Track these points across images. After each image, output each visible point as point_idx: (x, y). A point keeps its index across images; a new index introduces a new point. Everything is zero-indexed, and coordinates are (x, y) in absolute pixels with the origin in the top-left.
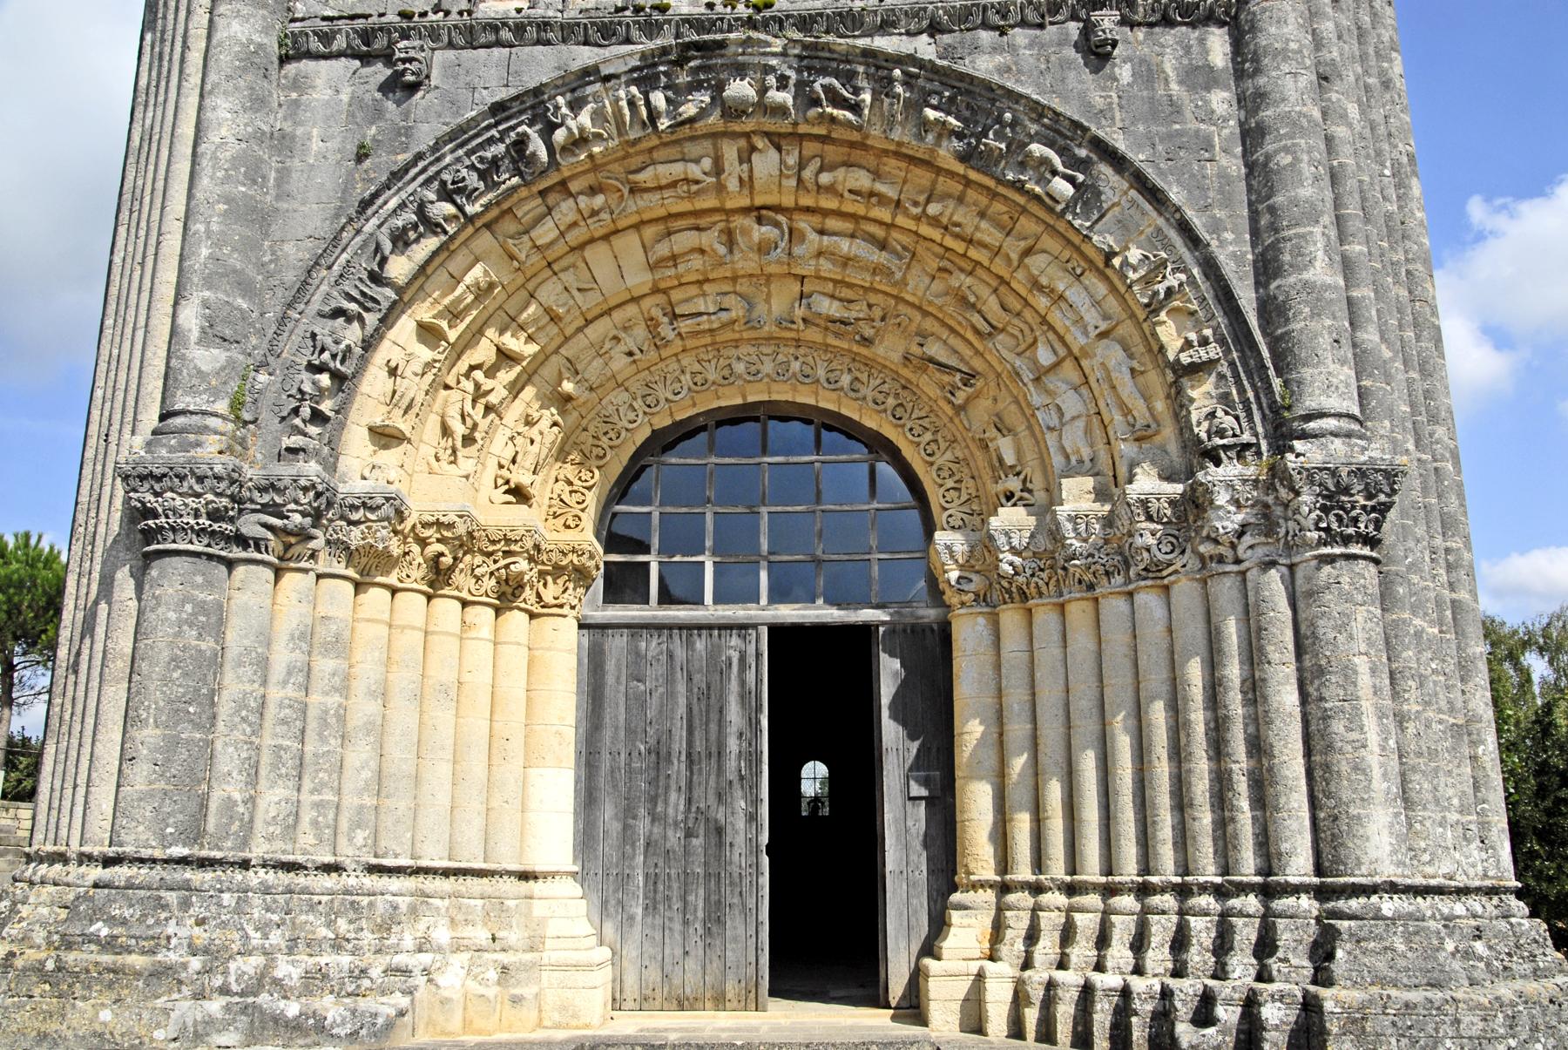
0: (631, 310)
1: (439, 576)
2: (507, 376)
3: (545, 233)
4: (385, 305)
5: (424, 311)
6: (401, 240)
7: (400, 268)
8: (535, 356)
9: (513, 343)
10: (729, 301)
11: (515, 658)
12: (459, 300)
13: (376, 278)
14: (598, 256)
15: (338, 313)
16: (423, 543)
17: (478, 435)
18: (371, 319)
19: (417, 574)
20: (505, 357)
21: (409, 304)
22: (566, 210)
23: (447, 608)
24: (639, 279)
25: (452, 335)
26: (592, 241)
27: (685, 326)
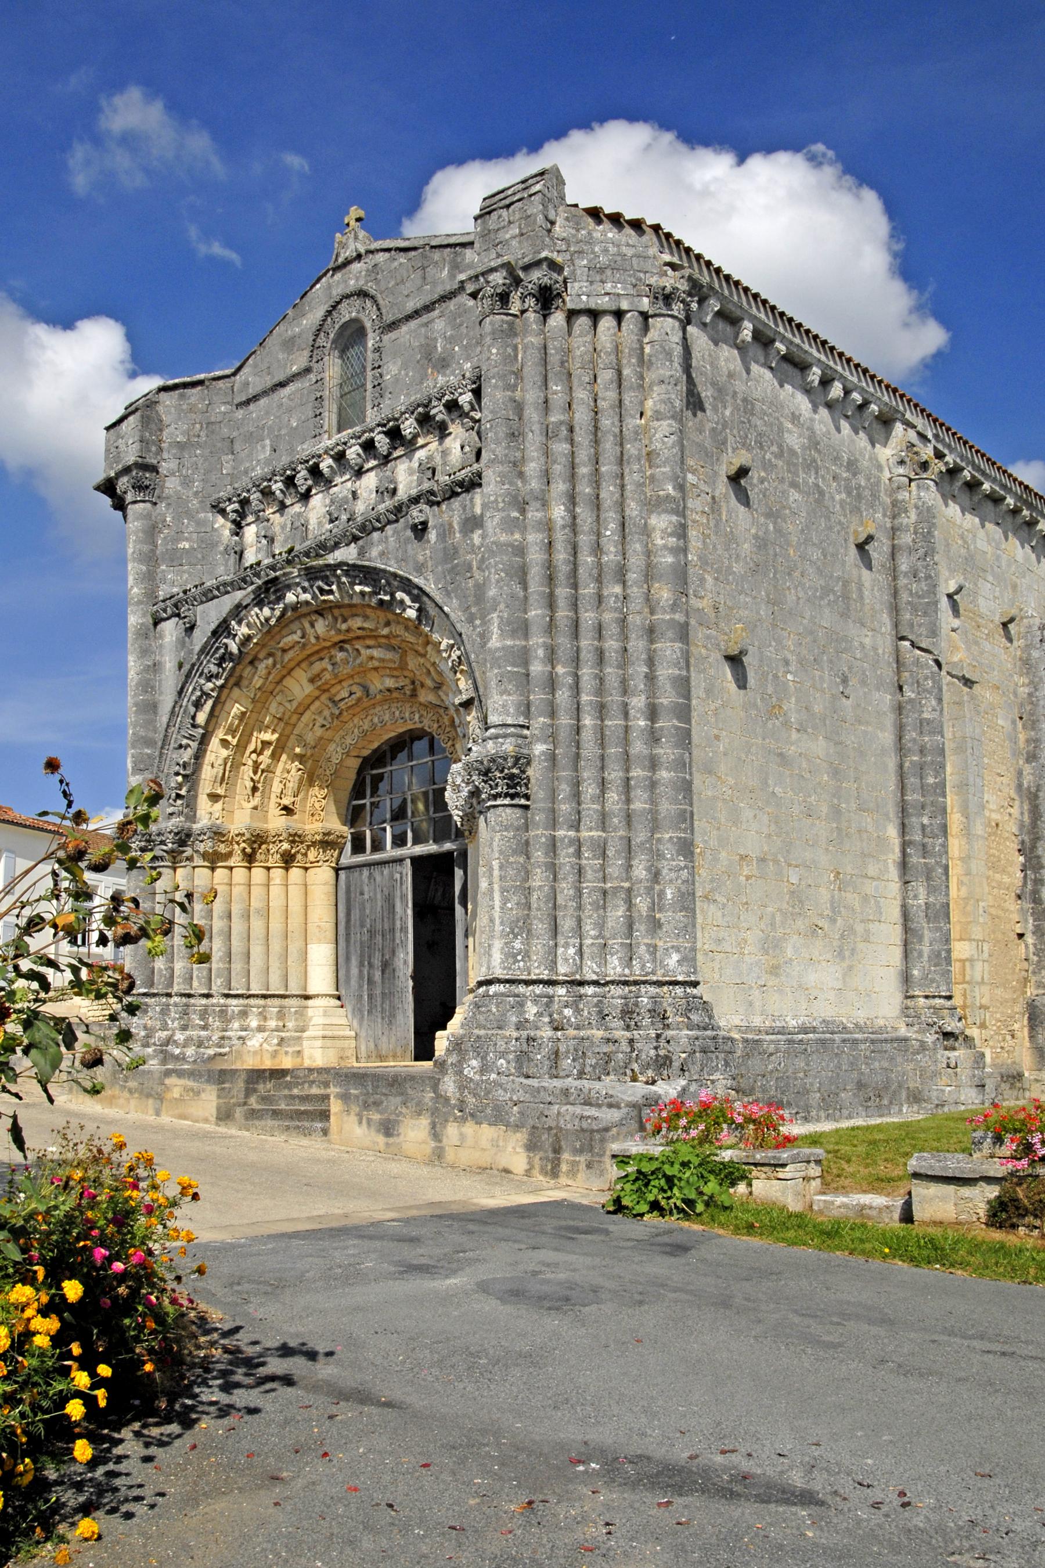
0: (317, 703)
1: (250, 858)
2: (268, 752)
3: (258, 682)
4: (199, 737)
5: (220, 734)
6: (198, 705)
7: (201, 718)
8: (278, 740)
9: (267, 736)
10: (355, 688)
11: (295, 892)
12: (232, 724)
13: (194, 726)
14: (288, 682)
15: (181, 746)
16: (238, 843)
17: (260, 785)
18: (194, 745)
19: (239, 858)
20: (266, 744)
21: (213, 732)
22: (262, 667)
23: (258, 874)
24: (309, 688)
25: (235, 742)
26: (284, 677)
27: (342, 705)
